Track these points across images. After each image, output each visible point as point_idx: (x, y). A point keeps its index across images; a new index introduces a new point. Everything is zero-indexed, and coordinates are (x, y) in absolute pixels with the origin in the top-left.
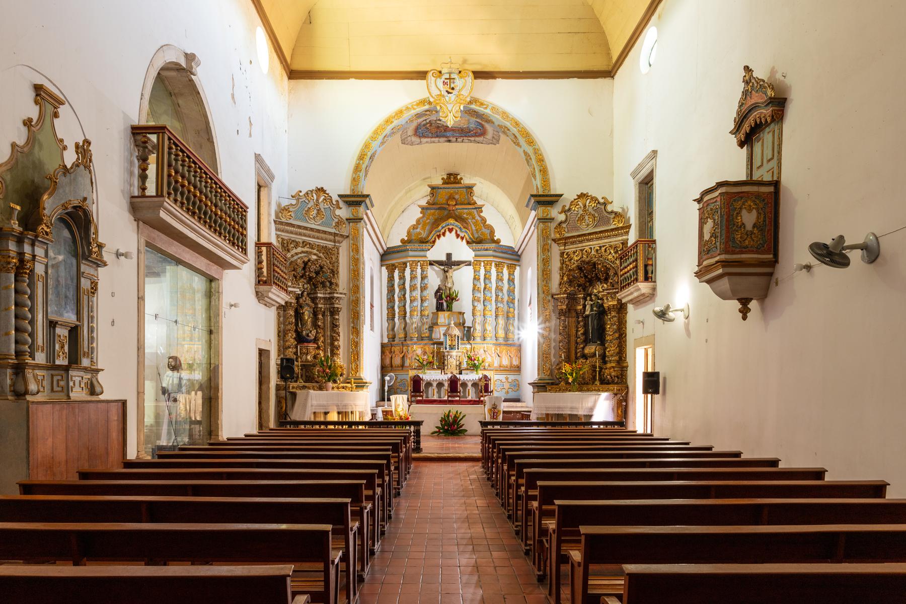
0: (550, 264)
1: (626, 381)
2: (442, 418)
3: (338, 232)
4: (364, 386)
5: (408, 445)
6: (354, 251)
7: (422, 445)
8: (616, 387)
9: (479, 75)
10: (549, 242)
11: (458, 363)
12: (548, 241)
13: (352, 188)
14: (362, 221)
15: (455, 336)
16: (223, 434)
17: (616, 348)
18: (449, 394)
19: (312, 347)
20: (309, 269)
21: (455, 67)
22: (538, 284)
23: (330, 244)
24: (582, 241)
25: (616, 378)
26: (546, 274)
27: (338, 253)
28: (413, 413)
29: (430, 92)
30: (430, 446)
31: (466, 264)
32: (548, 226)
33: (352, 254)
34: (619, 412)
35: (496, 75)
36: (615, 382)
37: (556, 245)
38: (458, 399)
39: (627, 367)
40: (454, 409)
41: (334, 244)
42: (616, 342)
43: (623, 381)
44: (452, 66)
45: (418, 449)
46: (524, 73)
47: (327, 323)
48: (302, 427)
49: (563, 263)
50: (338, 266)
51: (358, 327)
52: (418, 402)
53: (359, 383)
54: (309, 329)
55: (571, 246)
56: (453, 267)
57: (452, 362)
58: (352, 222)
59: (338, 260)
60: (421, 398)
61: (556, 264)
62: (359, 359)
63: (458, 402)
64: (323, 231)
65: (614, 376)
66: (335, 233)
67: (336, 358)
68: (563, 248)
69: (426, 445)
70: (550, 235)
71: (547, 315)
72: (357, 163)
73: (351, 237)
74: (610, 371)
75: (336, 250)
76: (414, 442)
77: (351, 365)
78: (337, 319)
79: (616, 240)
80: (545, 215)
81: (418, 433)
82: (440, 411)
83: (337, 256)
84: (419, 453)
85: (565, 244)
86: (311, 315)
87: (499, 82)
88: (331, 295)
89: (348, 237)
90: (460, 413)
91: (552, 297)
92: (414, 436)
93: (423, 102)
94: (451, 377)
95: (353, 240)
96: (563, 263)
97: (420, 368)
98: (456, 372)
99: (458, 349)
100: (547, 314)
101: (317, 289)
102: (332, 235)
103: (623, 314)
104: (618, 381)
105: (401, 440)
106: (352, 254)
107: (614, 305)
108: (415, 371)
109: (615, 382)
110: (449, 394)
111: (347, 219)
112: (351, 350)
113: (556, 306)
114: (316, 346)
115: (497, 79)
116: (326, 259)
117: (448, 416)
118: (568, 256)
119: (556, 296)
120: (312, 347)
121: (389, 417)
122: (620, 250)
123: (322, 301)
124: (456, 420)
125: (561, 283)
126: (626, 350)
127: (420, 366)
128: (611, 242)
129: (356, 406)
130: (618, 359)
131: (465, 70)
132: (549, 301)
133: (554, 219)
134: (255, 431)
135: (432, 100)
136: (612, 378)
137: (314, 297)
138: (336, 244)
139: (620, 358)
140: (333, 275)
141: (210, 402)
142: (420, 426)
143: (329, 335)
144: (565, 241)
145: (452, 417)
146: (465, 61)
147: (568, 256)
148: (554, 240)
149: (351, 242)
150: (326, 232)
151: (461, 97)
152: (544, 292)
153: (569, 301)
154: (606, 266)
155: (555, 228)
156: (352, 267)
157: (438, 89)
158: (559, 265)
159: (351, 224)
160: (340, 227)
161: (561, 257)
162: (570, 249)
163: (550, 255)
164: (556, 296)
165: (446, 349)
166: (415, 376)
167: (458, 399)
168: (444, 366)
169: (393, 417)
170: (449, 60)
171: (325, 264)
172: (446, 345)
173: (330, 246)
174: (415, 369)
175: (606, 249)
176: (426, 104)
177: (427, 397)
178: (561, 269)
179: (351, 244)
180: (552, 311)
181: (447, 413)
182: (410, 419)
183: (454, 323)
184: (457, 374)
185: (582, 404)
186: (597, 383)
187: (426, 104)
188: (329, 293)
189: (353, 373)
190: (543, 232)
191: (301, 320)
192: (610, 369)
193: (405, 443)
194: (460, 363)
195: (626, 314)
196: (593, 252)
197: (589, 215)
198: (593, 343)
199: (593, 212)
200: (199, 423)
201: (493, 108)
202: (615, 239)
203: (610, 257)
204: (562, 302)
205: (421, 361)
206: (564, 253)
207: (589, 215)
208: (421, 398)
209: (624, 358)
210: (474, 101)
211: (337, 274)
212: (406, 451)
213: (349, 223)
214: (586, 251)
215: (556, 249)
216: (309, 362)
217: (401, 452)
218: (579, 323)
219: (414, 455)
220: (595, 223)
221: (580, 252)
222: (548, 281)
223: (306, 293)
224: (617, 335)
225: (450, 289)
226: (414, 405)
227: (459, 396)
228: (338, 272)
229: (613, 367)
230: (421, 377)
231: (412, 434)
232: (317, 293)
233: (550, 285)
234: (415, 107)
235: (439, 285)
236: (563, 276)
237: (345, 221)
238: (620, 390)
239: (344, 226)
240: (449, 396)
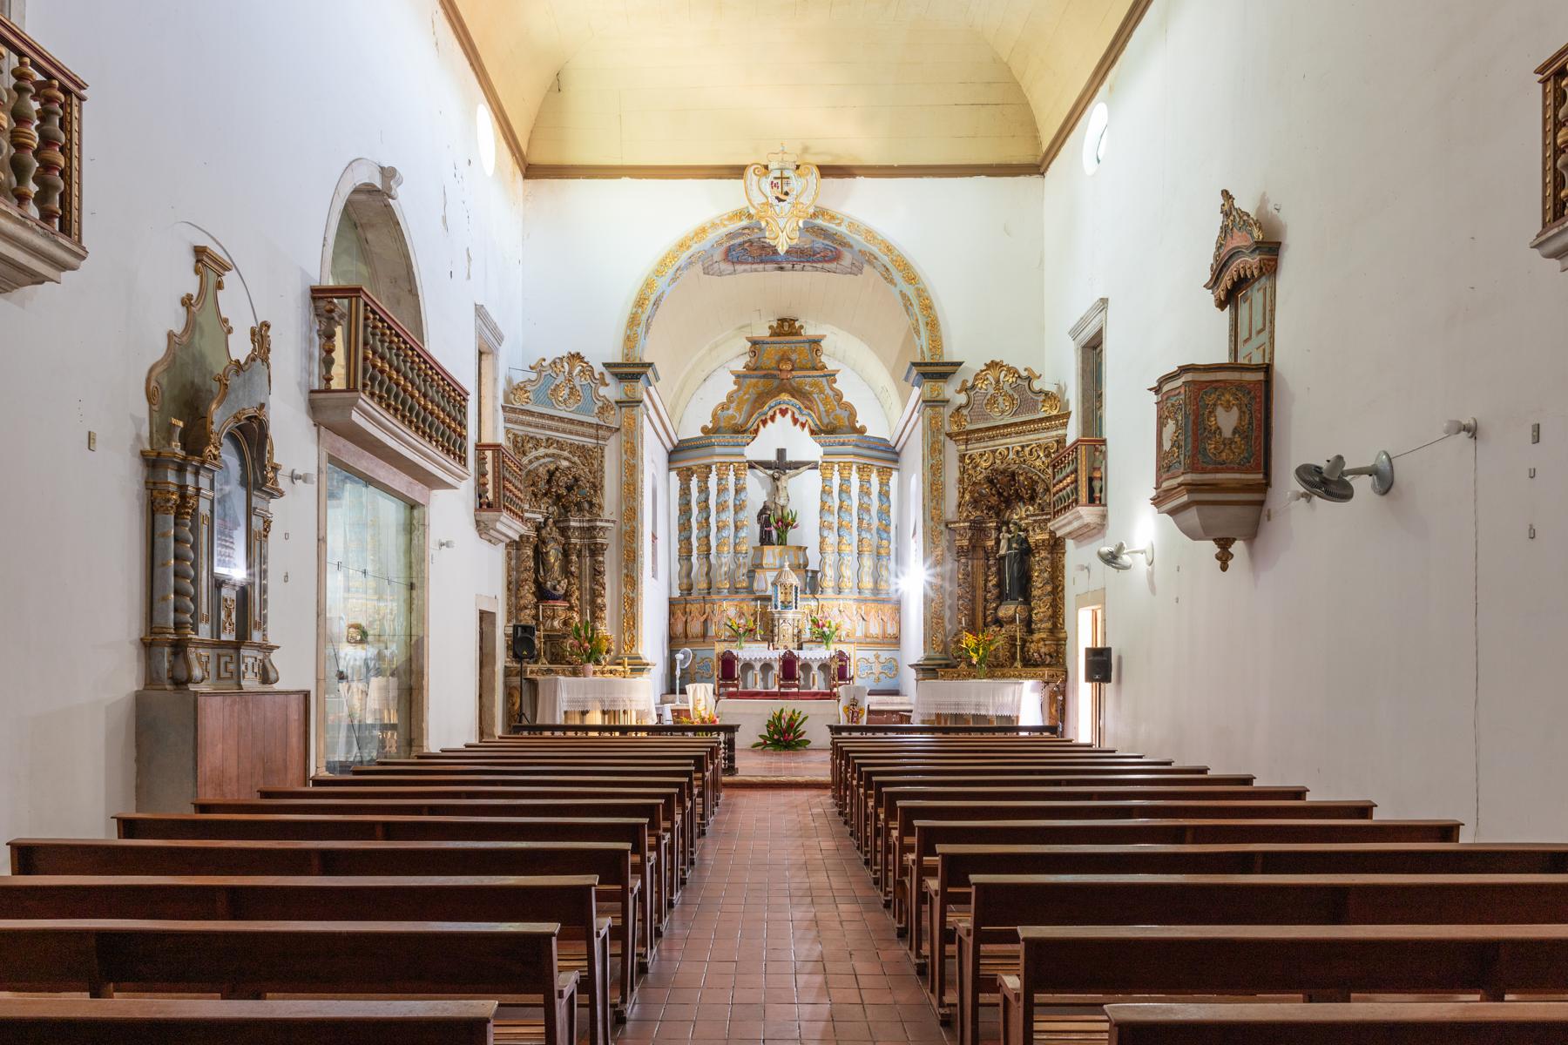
5: (716, 761)
7: (737, 764)
9: (827, 171)
16: (430, 743)
21: (791, 159)
28: (722, 713)
30: (750, 765)
31: (810, 466)
35: (856, 172)
44: (786, 157)
45: (731, 770)
46: (901, 167)
48: (548, 734)
52: (731, 695)
56: (787, 471)
60: (735, 689)
75: (599, 451)
76: (725, 759)
81: (730, 744)
84: (732, 775)
87: (861, 182)
92: (725, 749)
95: (625, 435)
97: (735, 639)
105: (707, 752)
108: (726, 644)
115: (858, 177)
121: (684, 719)
127: (733, 637)
131: (805, 164)
134: (474, 740)
140: (595, 491)
141: (411, 695)
142: (734, 732)
146: (806, 150)
151: (800, 206)
157: (763, 193)
166: (725, 653)
169: (690, 719)
170: (781, 149)
174: (725, 641)
177: (745, 687)
182: (718, 723)
193: (712, 759)
200: (393, 727)
201: (851, 224)
205: (735, 627)
208: (735, 689)
210: (820, 212)
211: (601, 489)
212: (713, 770)
213: (620, 408)
217: (707, 771)
219: (725, 779)
225: (783, 507)
226: (723, 700)
230: (735, 654)
231: (722, 745)
235: (765, 502)
237: (614, 405)
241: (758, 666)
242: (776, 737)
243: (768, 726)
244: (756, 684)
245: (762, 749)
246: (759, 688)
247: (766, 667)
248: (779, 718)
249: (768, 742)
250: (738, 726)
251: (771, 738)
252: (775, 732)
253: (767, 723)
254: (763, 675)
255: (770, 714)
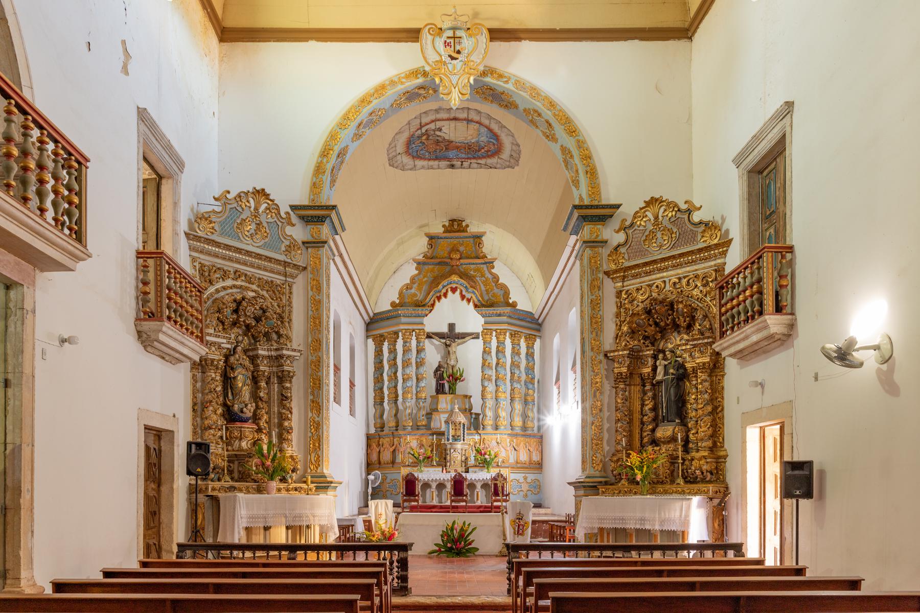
0: (601, 308)
1: (724, 476)
2: (443, 531)
3: (289, 261)
4: (328, 486)
6: (315, 290)
8: (711, 488)
10: (601, 275)
11: (463, 458)
12: (599, 275)
13: (312, 197)
14: (326, 245)
15: (460, 423)
17: (709, 428)
18: (453, 498)
19: (248, 428)
20: (245, 313)
22: (583, 339)
23: (278, 279)
24: (650, 272)
25: (708, 474)
26: (596, 323)
27: (291, 293)
29: (425, 58)
32: (599, 253)
33: (311, 293)
34: (716, 525)
36: (708, 479)
37: (610, 280)
38: (464, 504)
39: (726, 457)
40: (459, 519)
41: (284, 279)
42: (708, 419)
43: (718, 478)
47: (274, 394)
49: (620, 306)
50: (290, 312)
51: (320, 400)
53: (320, 483)
54: (244, 402)
55: (633, 282)
57: (456, 456)
58: (310, 247)
59: (291, 303)
61: (609, 308)
62: (321, 446)
63: (466, 510)
64: (267, 257)
65: (707, 471)
66: (285, 262)
67: (286, 446)
68: (620, 284)
69: (420, 577)
70: (601, 265)
71: (597, 383)
72: (319, 161)
73: (309, 268)
74: (700, 461)
77: (309, 456)
78: (287, 388)
79: (703, 268)
80: (593, 237)
82: (440, 522)
83: (289, 297)
85: (624, 279)
86: (249, 382)
88: (279, 353)
89: (305, 268)
90: (469, 525)
91: (606, 355)
93: (415, 73)
94: (456, 475)
96: (621, 307)
98: (461, 470)
99: (464, 440)
100: (598, 380)
101: (258, 343)
102: (280, 264)
103: (719, 377)
104: (711, 478)
106: (311, 293)
107: (704, 364)
109: (708, 479)
110: (453, 498)
111: (304, 243)
112: (310, 434)
113: (610, 370)
114: (256, 427)
116: (272, 299)
117: (452, 529)
118: (628, 296)
119: (612, 354)
120: (248, 428)
122: (711, 282)
123: (265, 362)
124: (462, 535)
125: (617, 335)
126: (723, 431)
128: (696, 270)
129: (314, 516)
130: (711, 445)
132: (600, 362)
133: (606, 242)
135: (427, 68)
136: (703, 473)
137: (253, 356)
138: (287, 279)
139: (715, 443)
143: (276, 411)
144: (624, 273)
145: (458, 531)
147: (628, 296)
148: (607, 273)
149: (310, 276)
150: (271, 258)
152: (592, 349)
153: (631, 363)
154: (690, 306)
155: (609, 256)
156: (310, 313)
158: (615, 309)
159: (310, 250)
160: (293, 253)
161: (617, 297)
162: (632, 284)
163: (601, 295)
164: (612, 354)
165: (448, 440)
167: (464, 504)
168: (446, 463)
171: (270, 306)
172: (449, 435)
173: (278, 282)
175: (688, 281)
176: (419, 76)
178: (618, 315)
179: (309, 280)
180: (604, 376)
181: (450, 525)
183: (458, 408)
184: (462, 472)
185: (660, 514)
186: (680, 481)
187: (419, 76)
188: (276, 350)
189: (312, 468)
190: (590, 261)
191: (231, 388)
192: (700, 459)
194: (466, 459)
195: (723, 376)
196: (668, 288)
197: (664, 230)
198: (668, 421)
199: (670, 226)
202: (703, 265)
203: (695, 292)
204: (621, 363)
206: (621, 291)
207: (664, 230)
209: (720, 443)
214: (657, 287)
215: (610, 287)
216: (243, 450)
218: (645, 393)
220: (673, 243)
221: (648, 288)
222: (599, 332)
223: (239, 348)
224: (709, 408)
227: (466, 501)
228: (291, 320)
229: (705, 457)
232: (256, 349)
233: (601, 339)
234: (404, 80)
236: (620, 326)
238: (717, 492)
239: (299, 252)
240: (452, 501)
241: (434, 485)
242: (449, 545)
243: (442, 536)
244: (433, 499)
245: (439, 554)
246: (435, 502)
247: (441, 486)
248: (452, 529)
249: (442, 550)
250: (412, 544)
251: (445, 546)
252: (448, 541)
253: (441, 533)
254: (439, 492)
255: (444, 526)
